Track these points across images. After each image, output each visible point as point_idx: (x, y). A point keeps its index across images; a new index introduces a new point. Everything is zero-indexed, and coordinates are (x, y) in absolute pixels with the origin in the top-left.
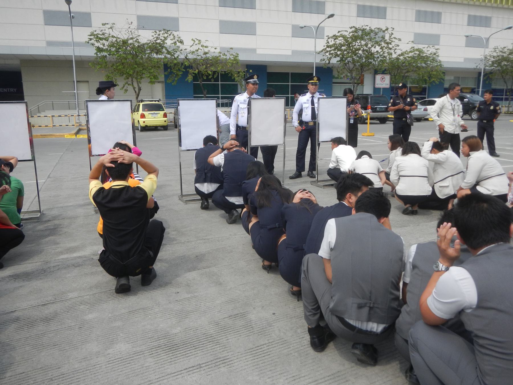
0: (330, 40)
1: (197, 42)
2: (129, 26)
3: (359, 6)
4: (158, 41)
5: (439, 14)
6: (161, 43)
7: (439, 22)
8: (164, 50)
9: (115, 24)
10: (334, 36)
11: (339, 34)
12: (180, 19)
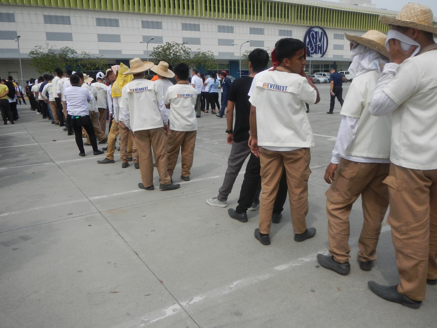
0: (155, 49)
1: (84, 53)
2: (48, 45)
3: (182, 24)
4: (64, 53)
5: (232, 28)
6: (66, 54)
7: (232, 32)
8: (68, 57)
9: (41, 46)
10: (157, 47)
11: (160, 46)
12: (72, 34)
